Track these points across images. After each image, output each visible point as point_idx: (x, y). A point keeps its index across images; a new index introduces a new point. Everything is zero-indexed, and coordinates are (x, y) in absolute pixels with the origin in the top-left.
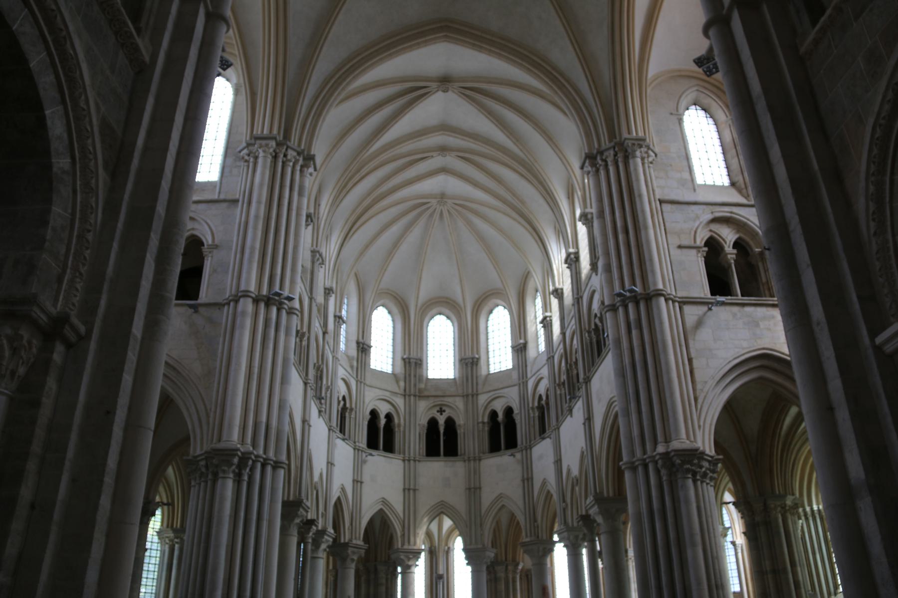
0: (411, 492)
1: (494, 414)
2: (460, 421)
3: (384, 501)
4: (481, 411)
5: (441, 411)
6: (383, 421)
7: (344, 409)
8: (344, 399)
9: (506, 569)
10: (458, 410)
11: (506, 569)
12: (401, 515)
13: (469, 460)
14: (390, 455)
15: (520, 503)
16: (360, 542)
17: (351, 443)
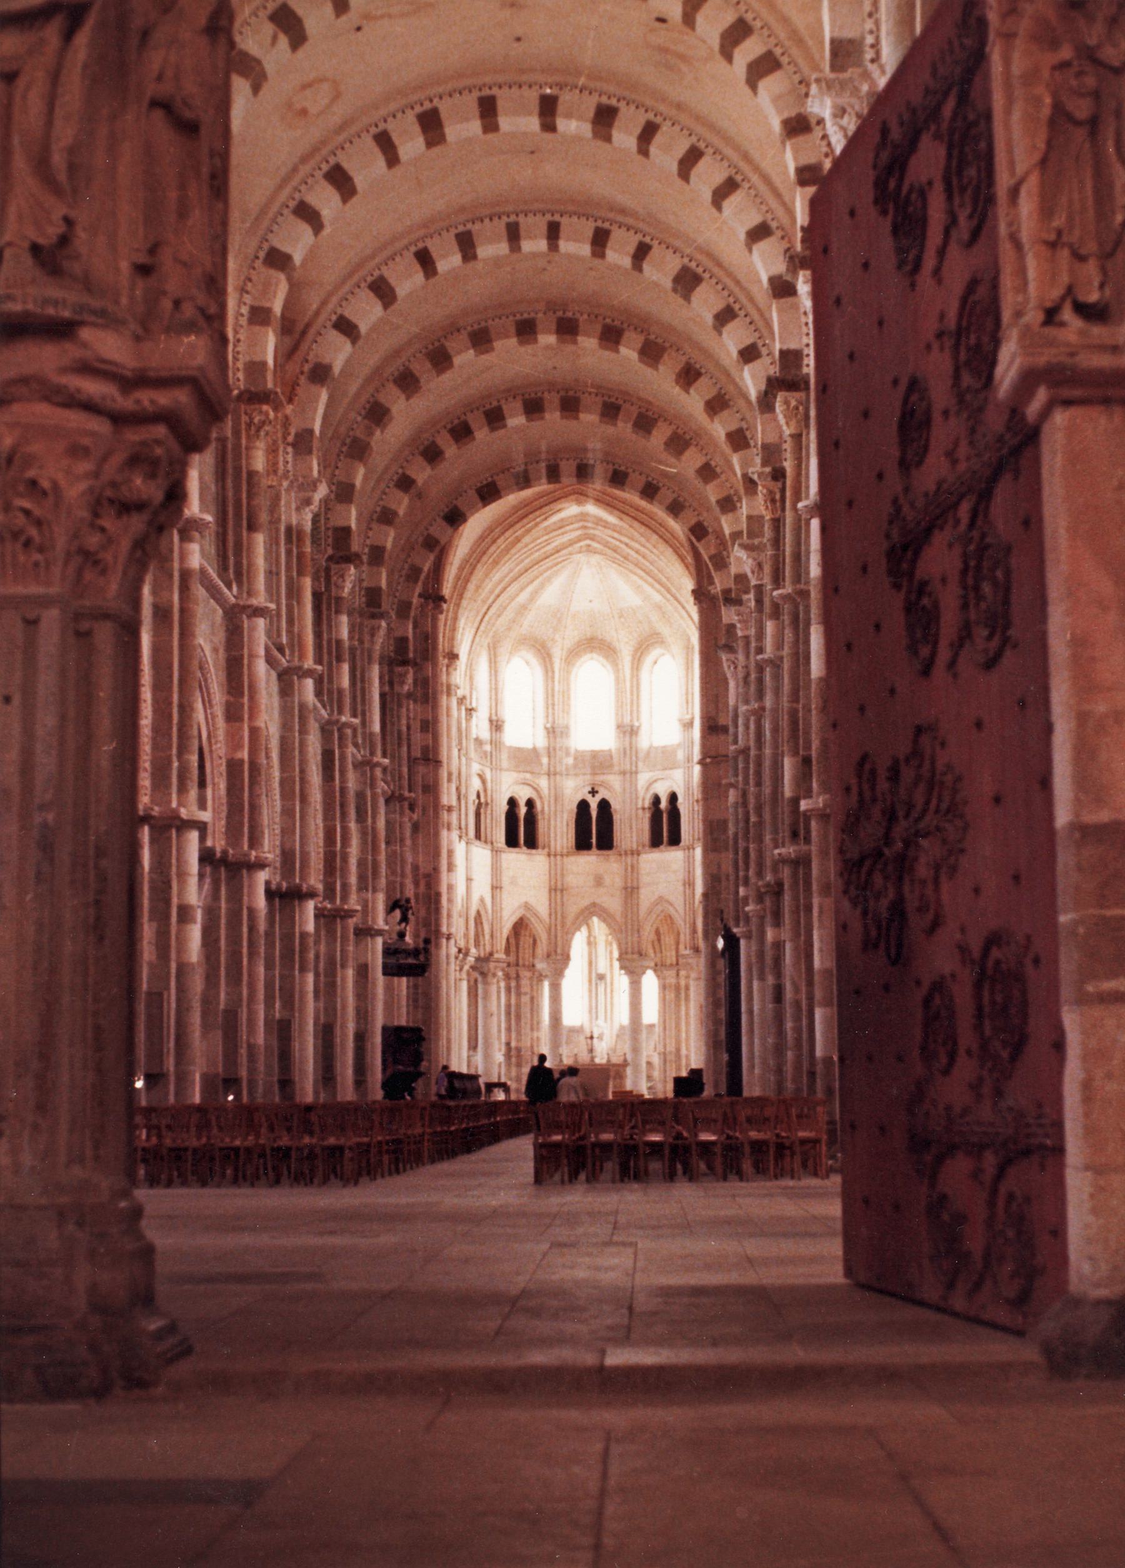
0: (558, 893)
1: (656, 800)
2: (615, 805)
3: (527, 906)
4: (641, 793)
5: (593, 792)
6: (523, 810)
7: (480, 804)
8: (478, 796)
9: (678, 975)
10: (614, 790)
11: (678, 975)
12: (547, 920)
13: (626, 854)
14: (534, 851)
15: (681, 910)
16: (502, 956)
17: (489, 846)
